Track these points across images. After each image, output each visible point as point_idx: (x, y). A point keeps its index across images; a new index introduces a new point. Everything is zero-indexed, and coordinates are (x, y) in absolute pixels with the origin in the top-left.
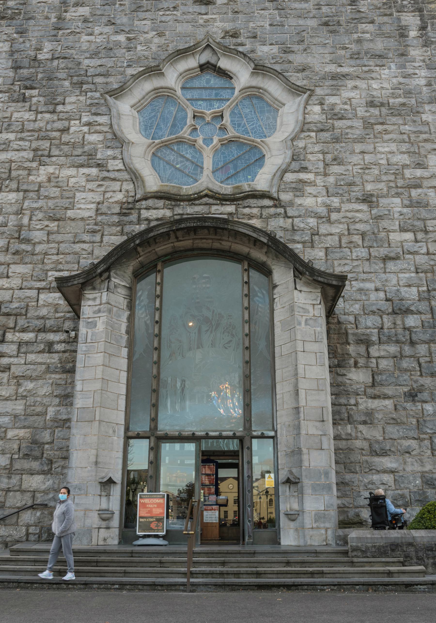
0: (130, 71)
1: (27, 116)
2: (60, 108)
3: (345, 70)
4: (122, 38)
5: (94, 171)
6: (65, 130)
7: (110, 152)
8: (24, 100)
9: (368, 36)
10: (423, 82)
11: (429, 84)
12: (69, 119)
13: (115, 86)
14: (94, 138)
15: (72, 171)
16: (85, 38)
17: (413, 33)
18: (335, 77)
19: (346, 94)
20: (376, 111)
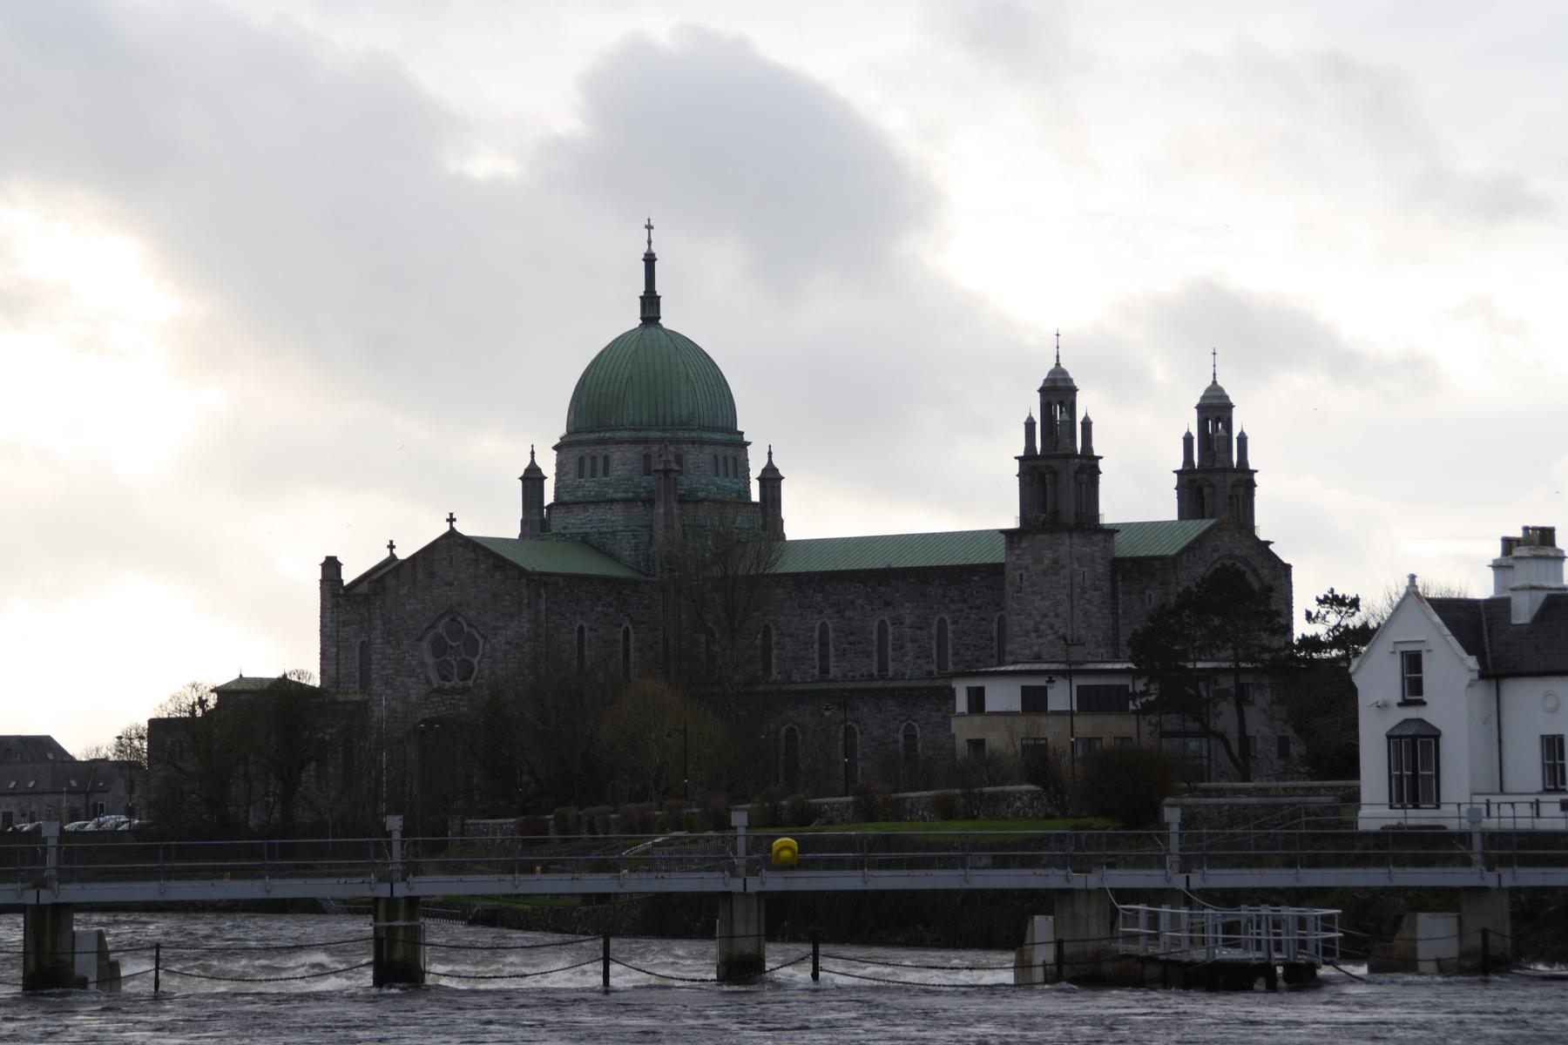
0: (425, 627)
1: (391, 651)
2: (402, 647)
3: (499, 624)
4: (419, 607)
5: (414, 679)
6: (404, 659)
7: (419, 670)
8: (389, 642)
9: (508, 603)
10: (525, 630)
11: (528, 631)
12: (405, 653)
13: (420, 635)
14: (414, 663)
15: (407, 680)
16: (408, 607)
17: (525, 601)
18: (496, 628)
19: (499, 638)
20: (508, 647)
